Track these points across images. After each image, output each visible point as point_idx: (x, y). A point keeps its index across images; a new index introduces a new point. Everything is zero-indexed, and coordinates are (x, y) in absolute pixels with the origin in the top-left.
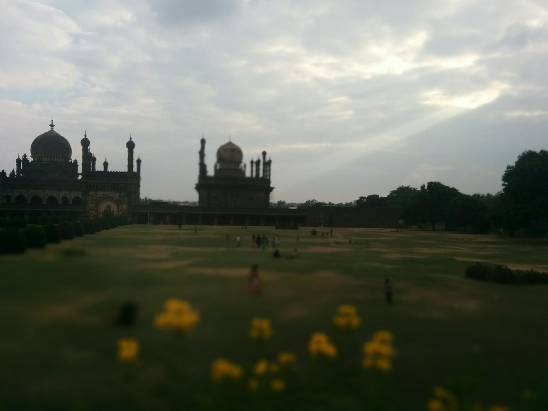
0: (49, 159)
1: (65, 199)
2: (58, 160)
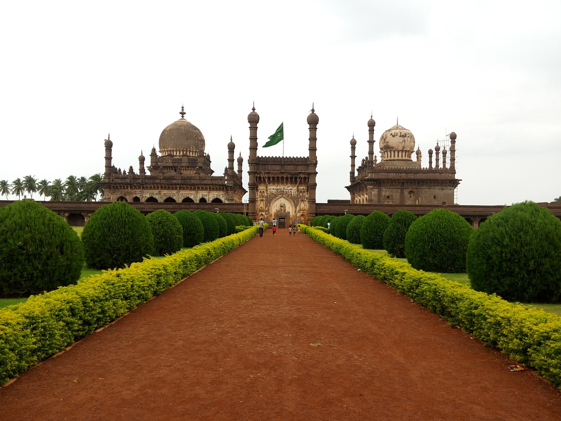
0: (181, 154)
1: (203, 200)
2: (191, 154)
